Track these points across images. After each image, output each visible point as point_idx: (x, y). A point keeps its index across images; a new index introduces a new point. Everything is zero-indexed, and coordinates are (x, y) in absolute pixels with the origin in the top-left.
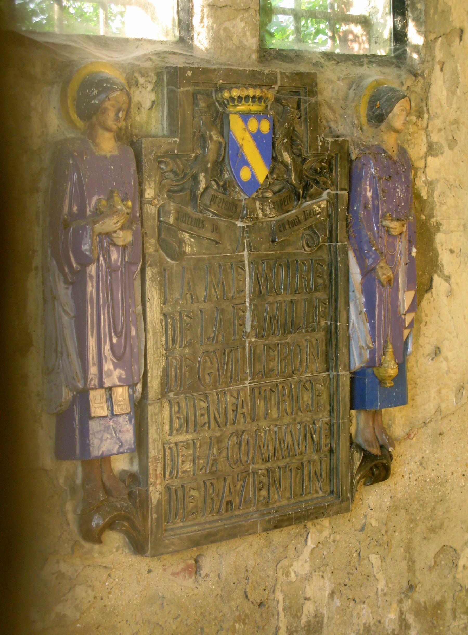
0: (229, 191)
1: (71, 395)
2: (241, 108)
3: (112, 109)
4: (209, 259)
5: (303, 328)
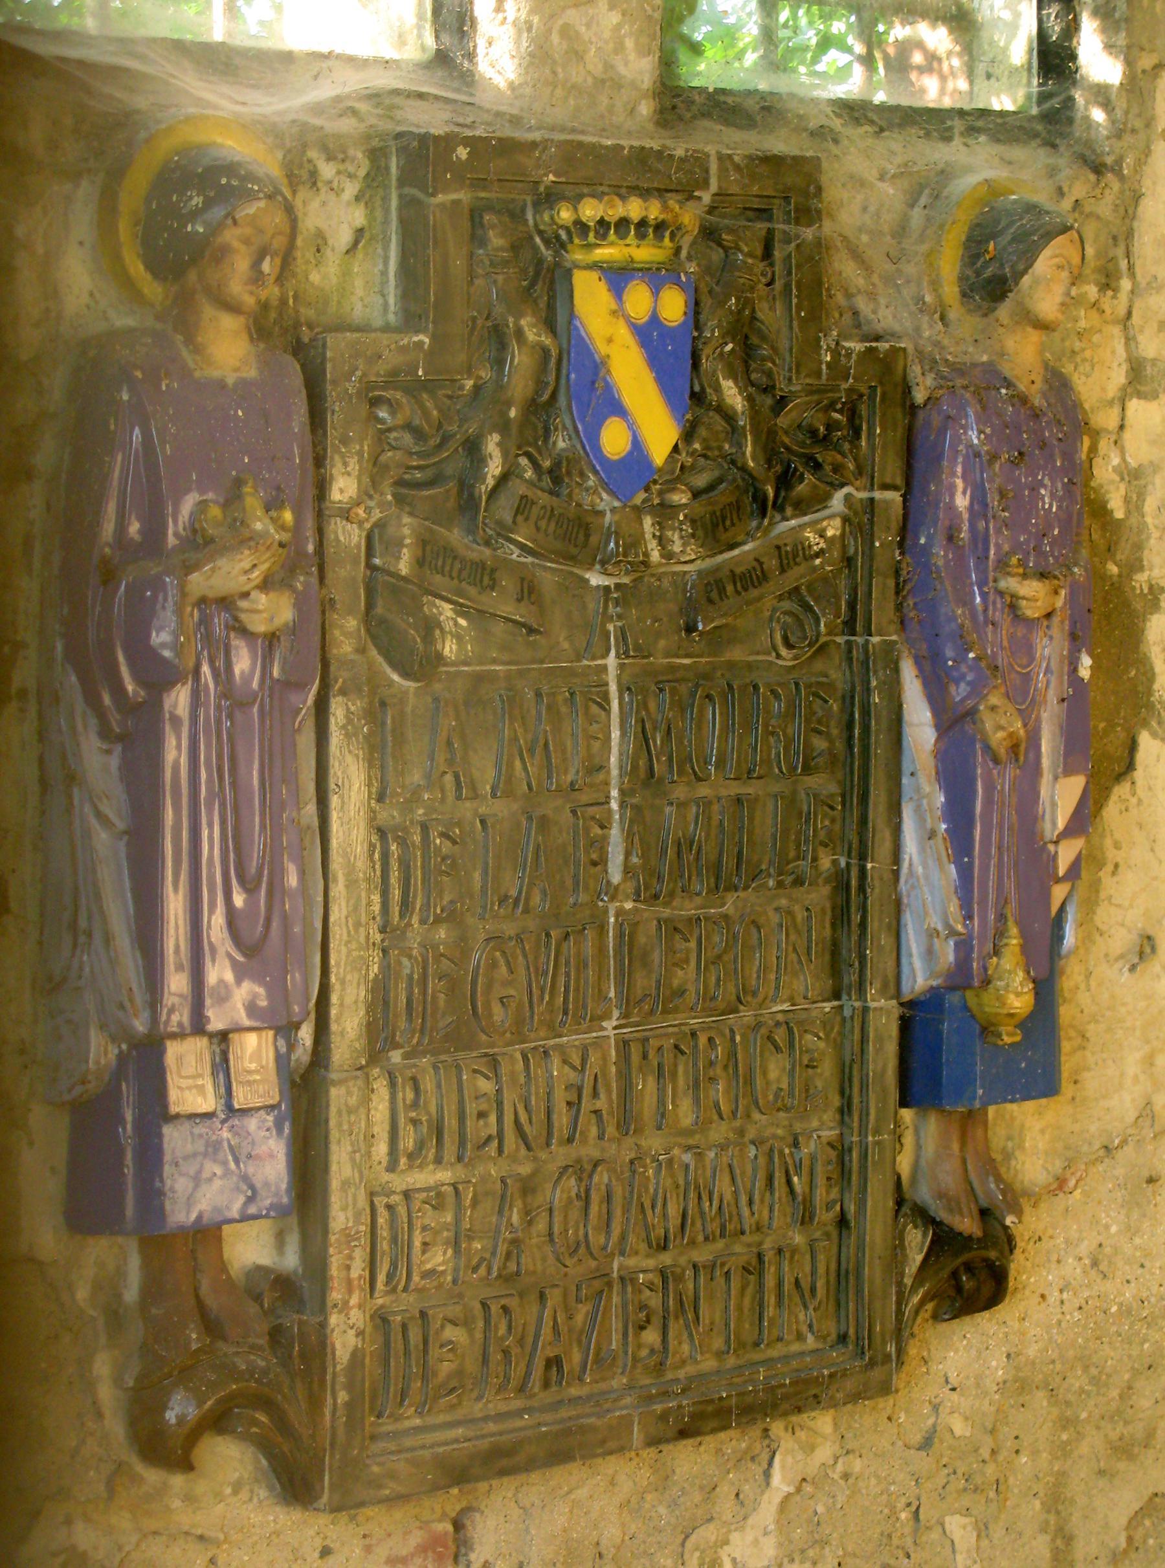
1: (113, 1052)
2: (603, 253)
3: (243, 248)
4: (508, 676)
5: (769, 875)
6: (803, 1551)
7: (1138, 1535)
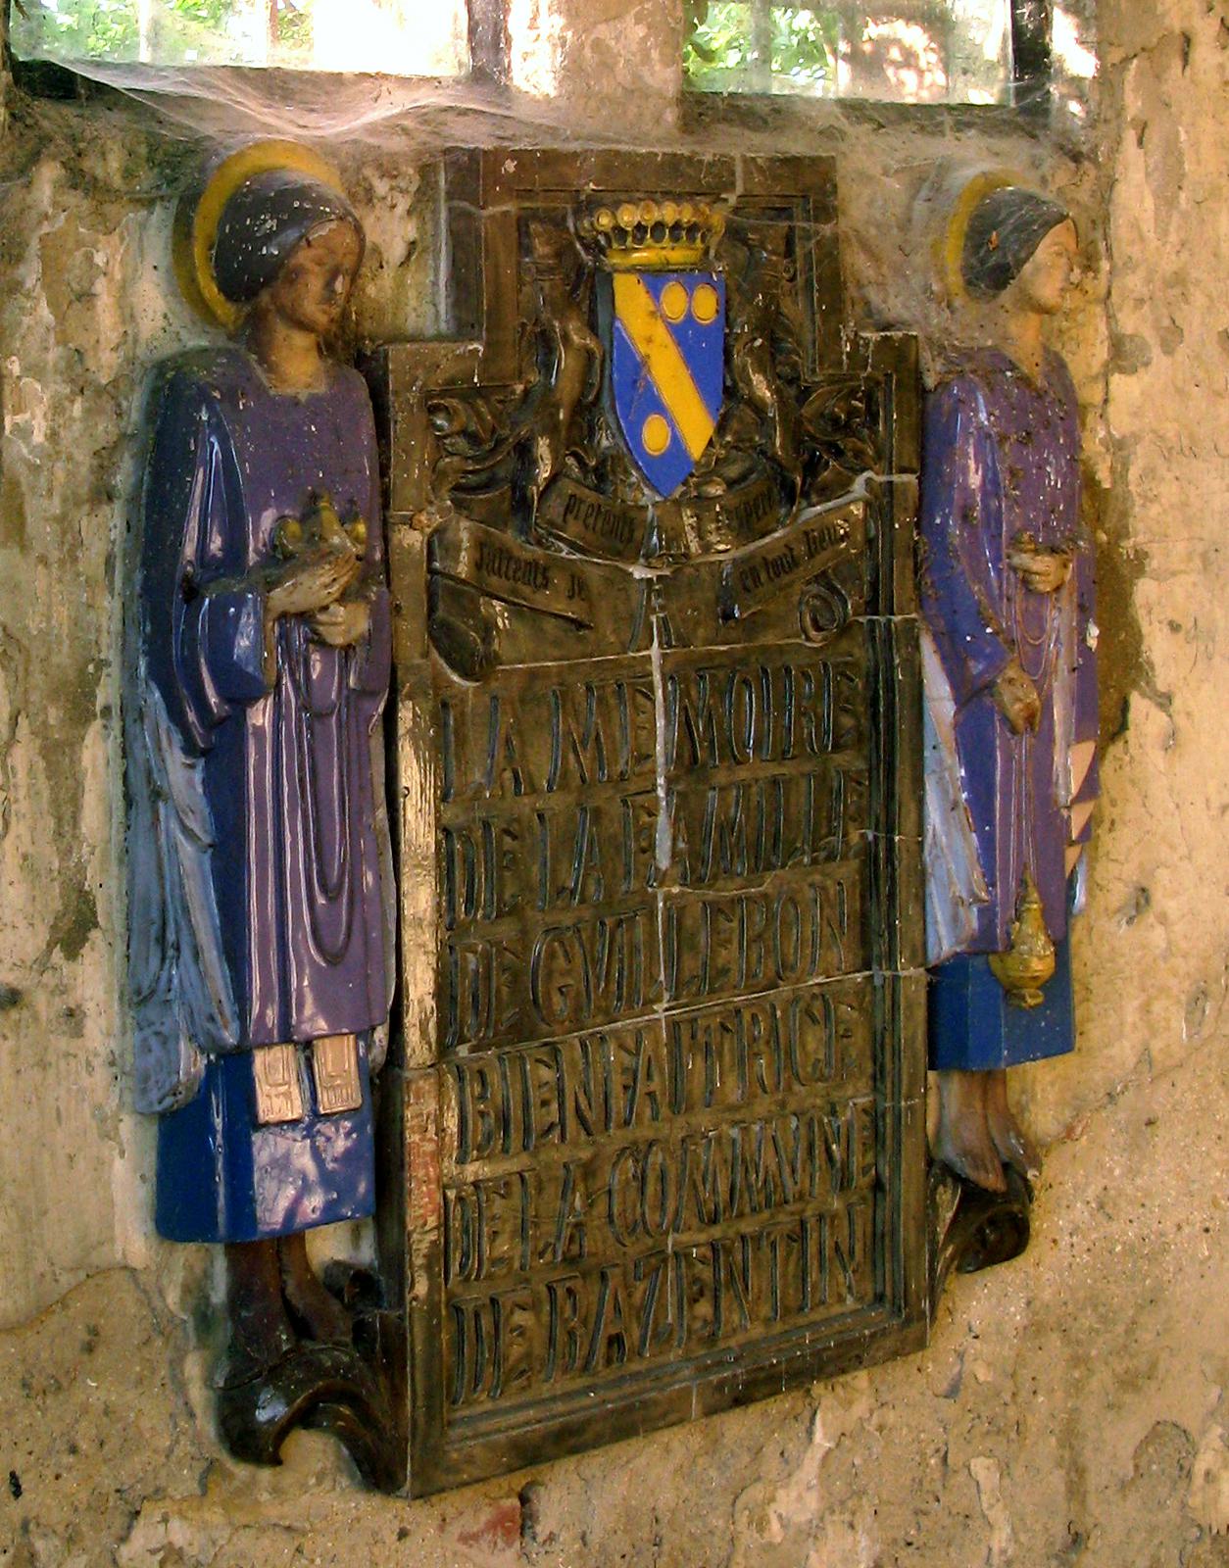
0: (613, 483)
1: (202, 1062)
2: (640, 256)
3: (317, 269)
5: (803, 853)
6: (842, 1503)
7: (1143, 1463)
